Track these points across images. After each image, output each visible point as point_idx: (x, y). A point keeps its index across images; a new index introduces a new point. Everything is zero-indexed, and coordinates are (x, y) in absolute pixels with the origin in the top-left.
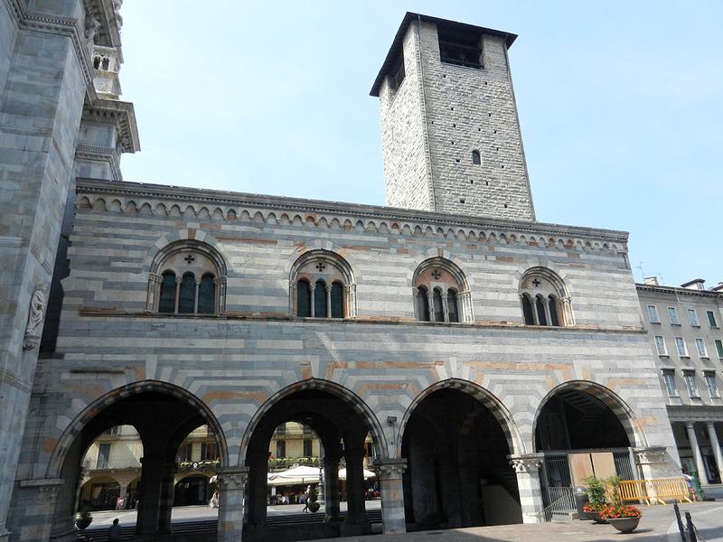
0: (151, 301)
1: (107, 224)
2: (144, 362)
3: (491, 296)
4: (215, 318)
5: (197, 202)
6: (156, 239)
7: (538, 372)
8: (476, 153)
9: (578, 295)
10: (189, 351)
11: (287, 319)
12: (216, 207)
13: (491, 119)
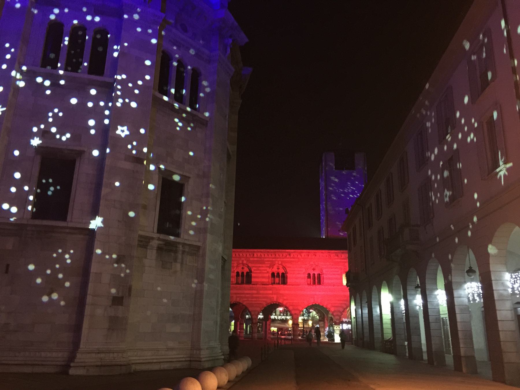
10: (242, 294)
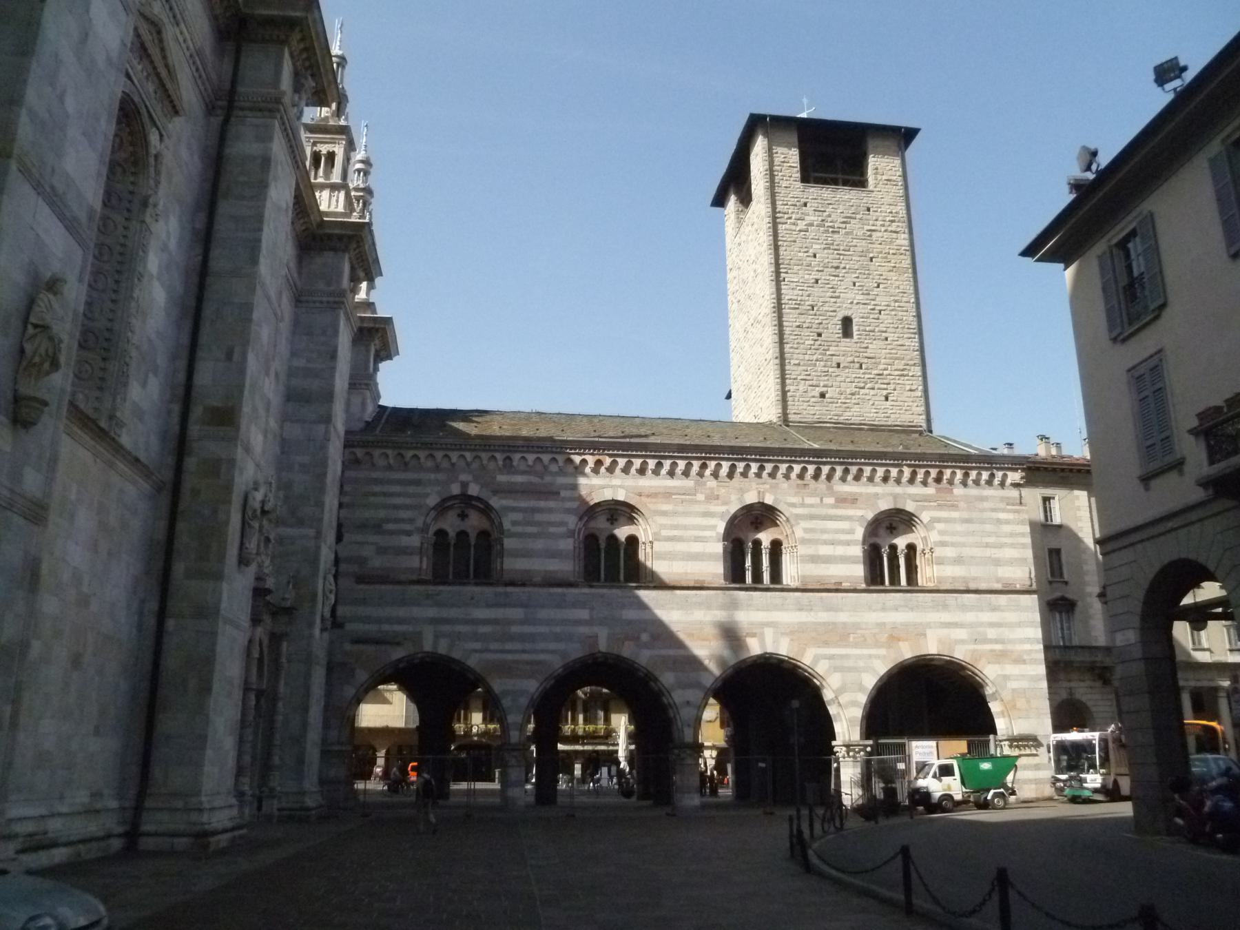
0: (424, 567)
1: (376, 481)
2: (420, 633)
3: (824, 550)
4: (491, 584)
5: (469, 450)
6: (427, 495)
7: (877, 645)
8: (847, 323)
9: (943, 544)
11: (571, 585)
12: (490, 454)
13: (873, 266)
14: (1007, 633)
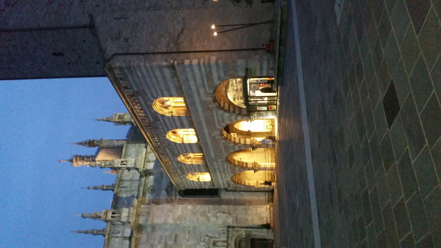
14: (198, 77)
